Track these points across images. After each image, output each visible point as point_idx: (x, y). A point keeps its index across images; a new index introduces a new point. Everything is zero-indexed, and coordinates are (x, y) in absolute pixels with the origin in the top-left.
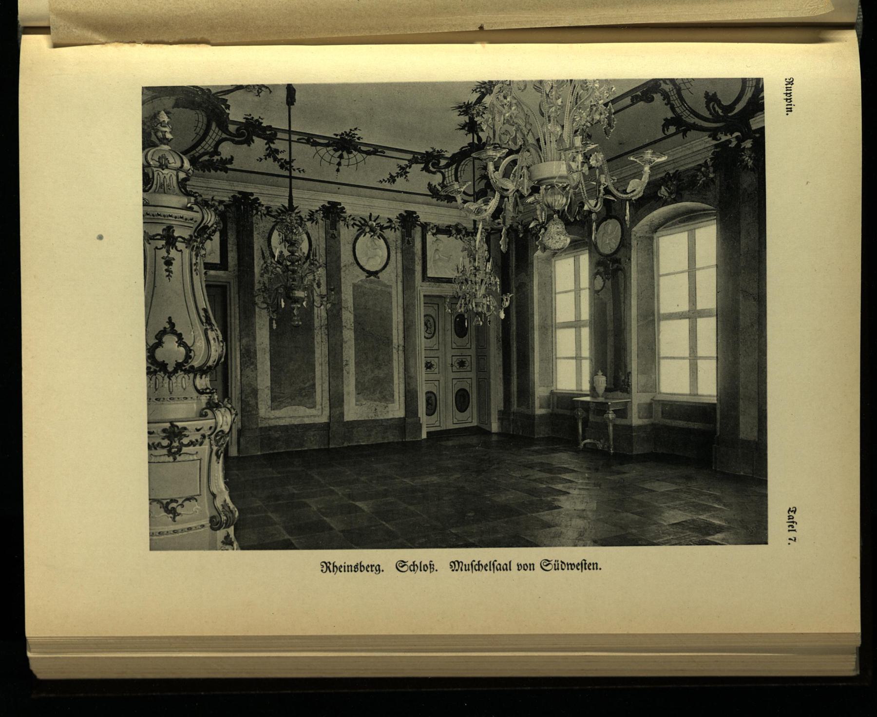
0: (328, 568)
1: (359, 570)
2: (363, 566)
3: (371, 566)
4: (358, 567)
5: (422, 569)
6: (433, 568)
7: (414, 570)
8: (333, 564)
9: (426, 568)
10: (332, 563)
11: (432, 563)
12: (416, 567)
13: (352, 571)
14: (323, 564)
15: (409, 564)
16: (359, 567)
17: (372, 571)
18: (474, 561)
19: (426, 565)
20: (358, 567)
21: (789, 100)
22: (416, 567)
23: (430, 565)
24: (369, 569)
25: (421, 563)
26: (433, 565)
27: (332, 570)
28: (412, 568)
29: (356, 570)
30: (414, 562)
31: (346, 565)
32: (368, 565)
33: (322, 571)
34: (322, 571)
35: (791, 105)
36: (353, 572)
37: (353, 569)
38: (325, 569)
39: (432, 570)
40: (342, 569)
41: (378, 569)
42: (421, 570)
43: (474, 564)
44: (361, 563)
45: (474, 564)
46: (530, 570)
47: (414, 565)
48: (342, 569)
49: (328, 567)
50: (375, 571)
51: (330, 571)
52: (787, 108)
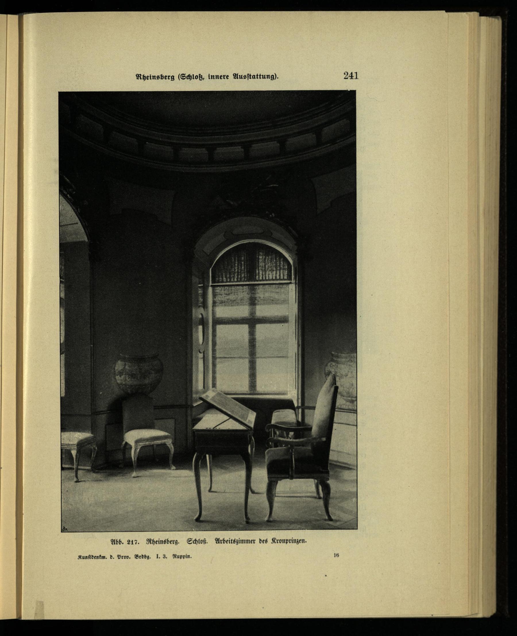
3: (173, 541)
6: (205, 542)
7: (196, 543)
10: (152, 539)
16: (166, 541)
17: (173, 543)
23: (204, 541)
25: (199, 540)
26: (206, 540)
28: (194, 542)
31: (160, 540)
34: (147, 543)
35: (150, 77)
36: (164, 544)
37: (163, 543)
41: (176, 543)
42: (199, 543)
47: (195, 540)
50: (175, 544)
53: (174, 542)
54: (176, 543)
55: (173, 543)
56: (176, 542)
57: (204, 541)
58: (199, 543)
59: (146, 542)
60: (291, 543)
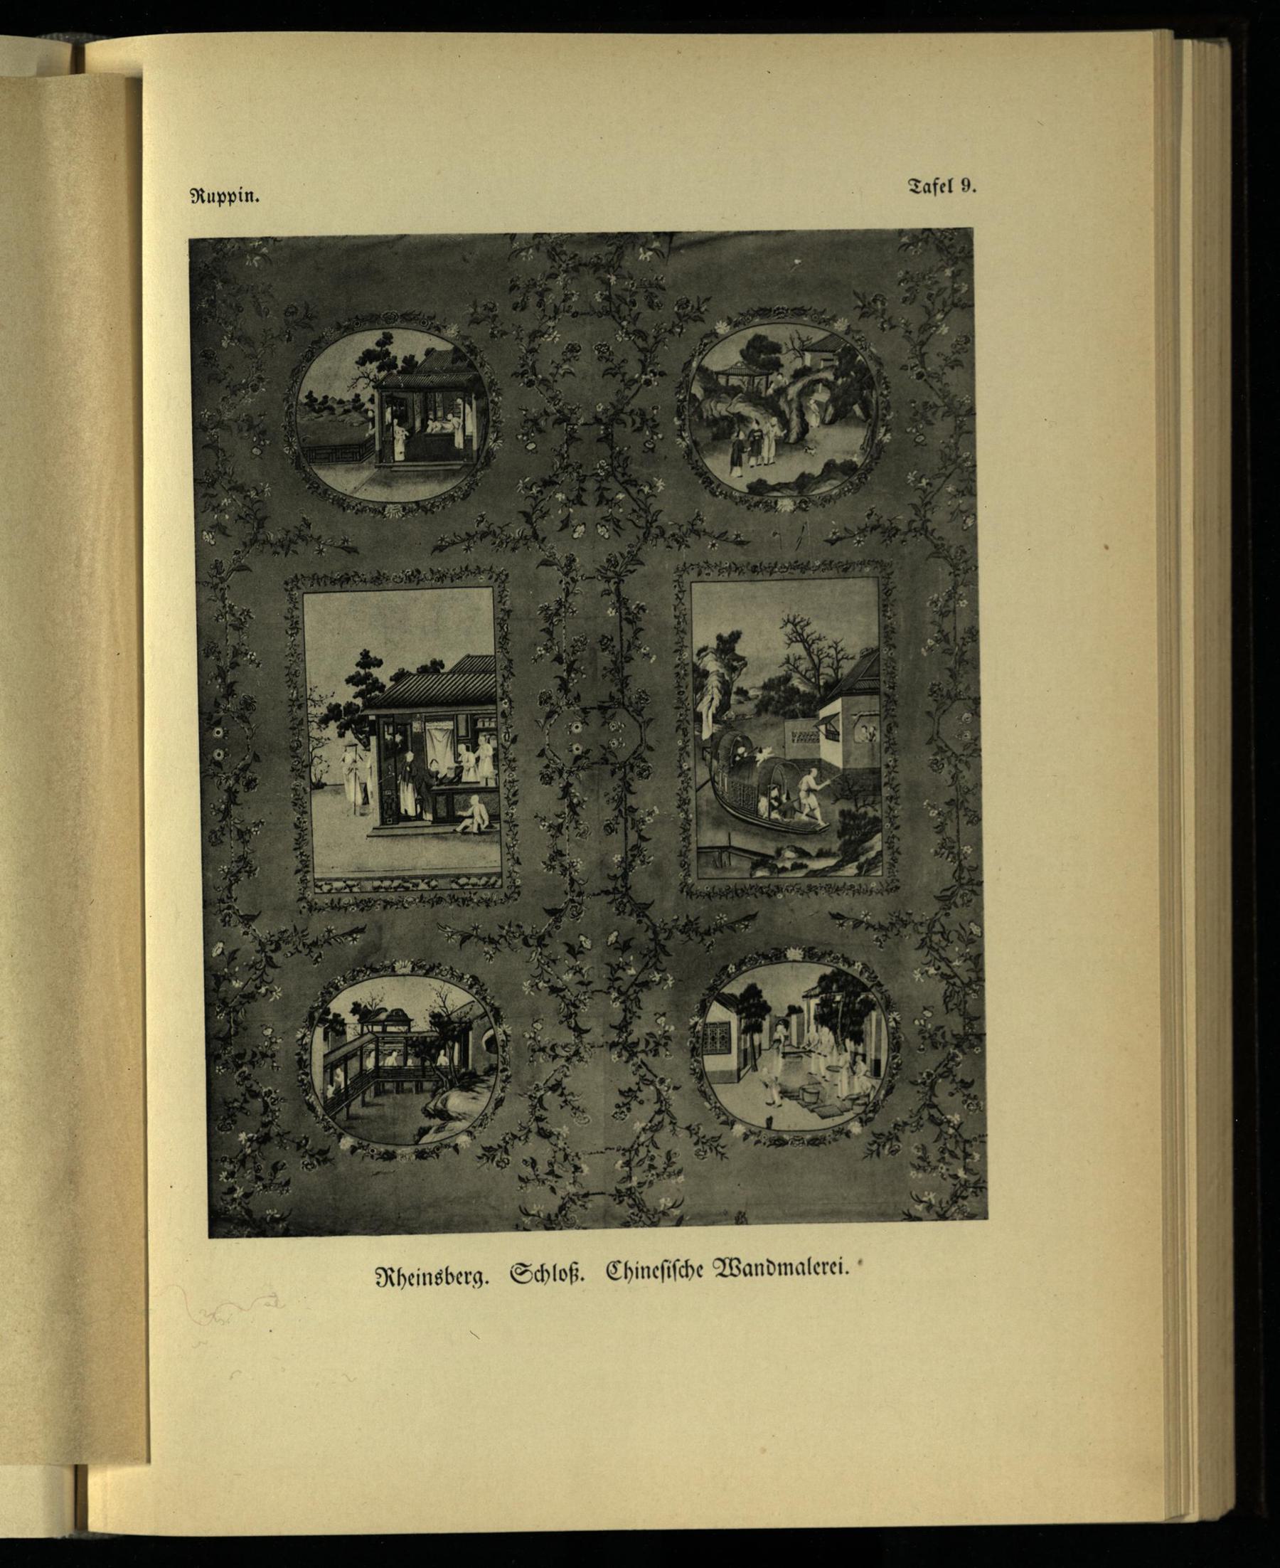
0: (389, 1278)
1: (444, 1280)
2: (451, 1274)
3: (466, 1273)
4: (444, 1277)
5: (558, 1277)
6: (576, 1276)
8: (399, 1271)
9: (563, 1276)
10: (396, 1269)
11: (574, 1267)
12: (546, 1275)
13: (431, 1283)
14: (381, 1271)
15: (533, 1269)
16: (444, 1276)
17: (467, 1282)
18: (678, 1260)
19: (564, 1270)
20: (444, 1277)
21: (231, 198)
22: (546, 1275)
23: (571, 1270)
24: (462, 1279)
25: (554, 1267)
26: (577, 1270)
27: (395, 1281)
29: (439, 1281)
30: (542, 1266)
31: (421, 1273)
32: (460, 1273)
33: (378, 1283)
34: (378, 1283)
37: (434, 1280)
38: (383, 1280)
39: (574, 1278)
40: (414, 1281)
41: (479, 1279)
43: (678, 1265)
44: (447, 1269)
45: (678, 1265)
46: (780, 1274)
47: (542, 1269)
48: (414, 1281)
49: (388, 1276)
50: (472, 1283)
51: (393, 1284)
52: (247, 200)
53: (470, 1278)
54: (479, 1279)
55: (467, 1282)
56: (477, 1277)
57: (572, 1273)
58: (555, 1280)
59: (374, 1278)
60: (821, 1274)
